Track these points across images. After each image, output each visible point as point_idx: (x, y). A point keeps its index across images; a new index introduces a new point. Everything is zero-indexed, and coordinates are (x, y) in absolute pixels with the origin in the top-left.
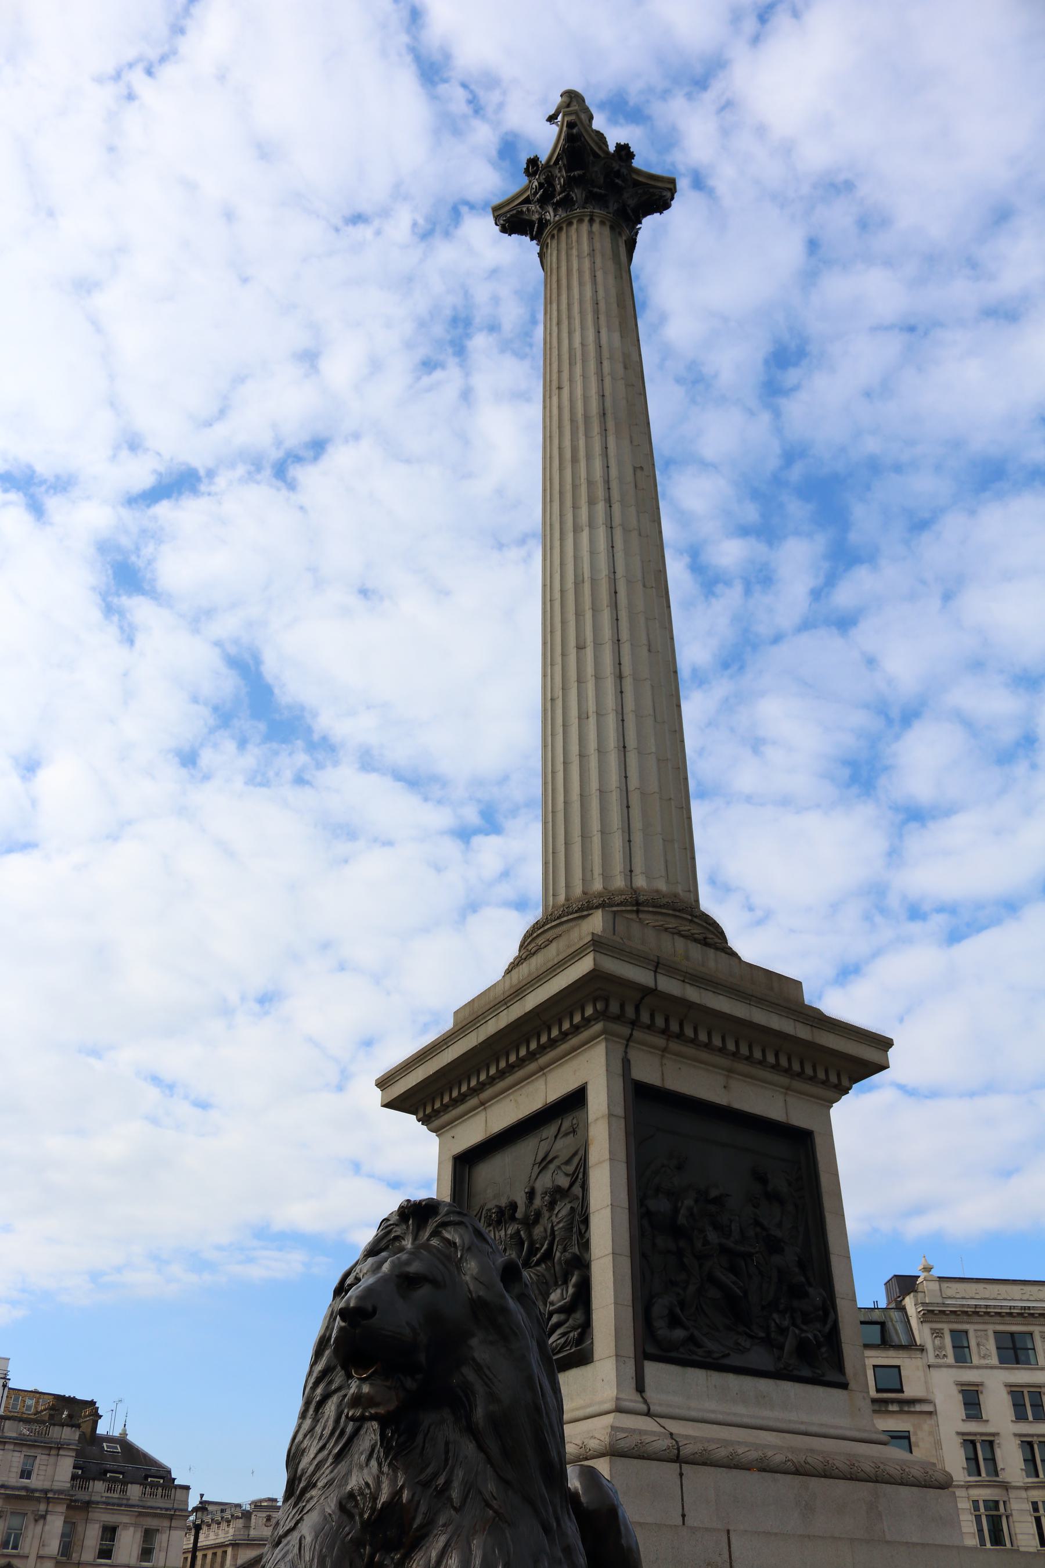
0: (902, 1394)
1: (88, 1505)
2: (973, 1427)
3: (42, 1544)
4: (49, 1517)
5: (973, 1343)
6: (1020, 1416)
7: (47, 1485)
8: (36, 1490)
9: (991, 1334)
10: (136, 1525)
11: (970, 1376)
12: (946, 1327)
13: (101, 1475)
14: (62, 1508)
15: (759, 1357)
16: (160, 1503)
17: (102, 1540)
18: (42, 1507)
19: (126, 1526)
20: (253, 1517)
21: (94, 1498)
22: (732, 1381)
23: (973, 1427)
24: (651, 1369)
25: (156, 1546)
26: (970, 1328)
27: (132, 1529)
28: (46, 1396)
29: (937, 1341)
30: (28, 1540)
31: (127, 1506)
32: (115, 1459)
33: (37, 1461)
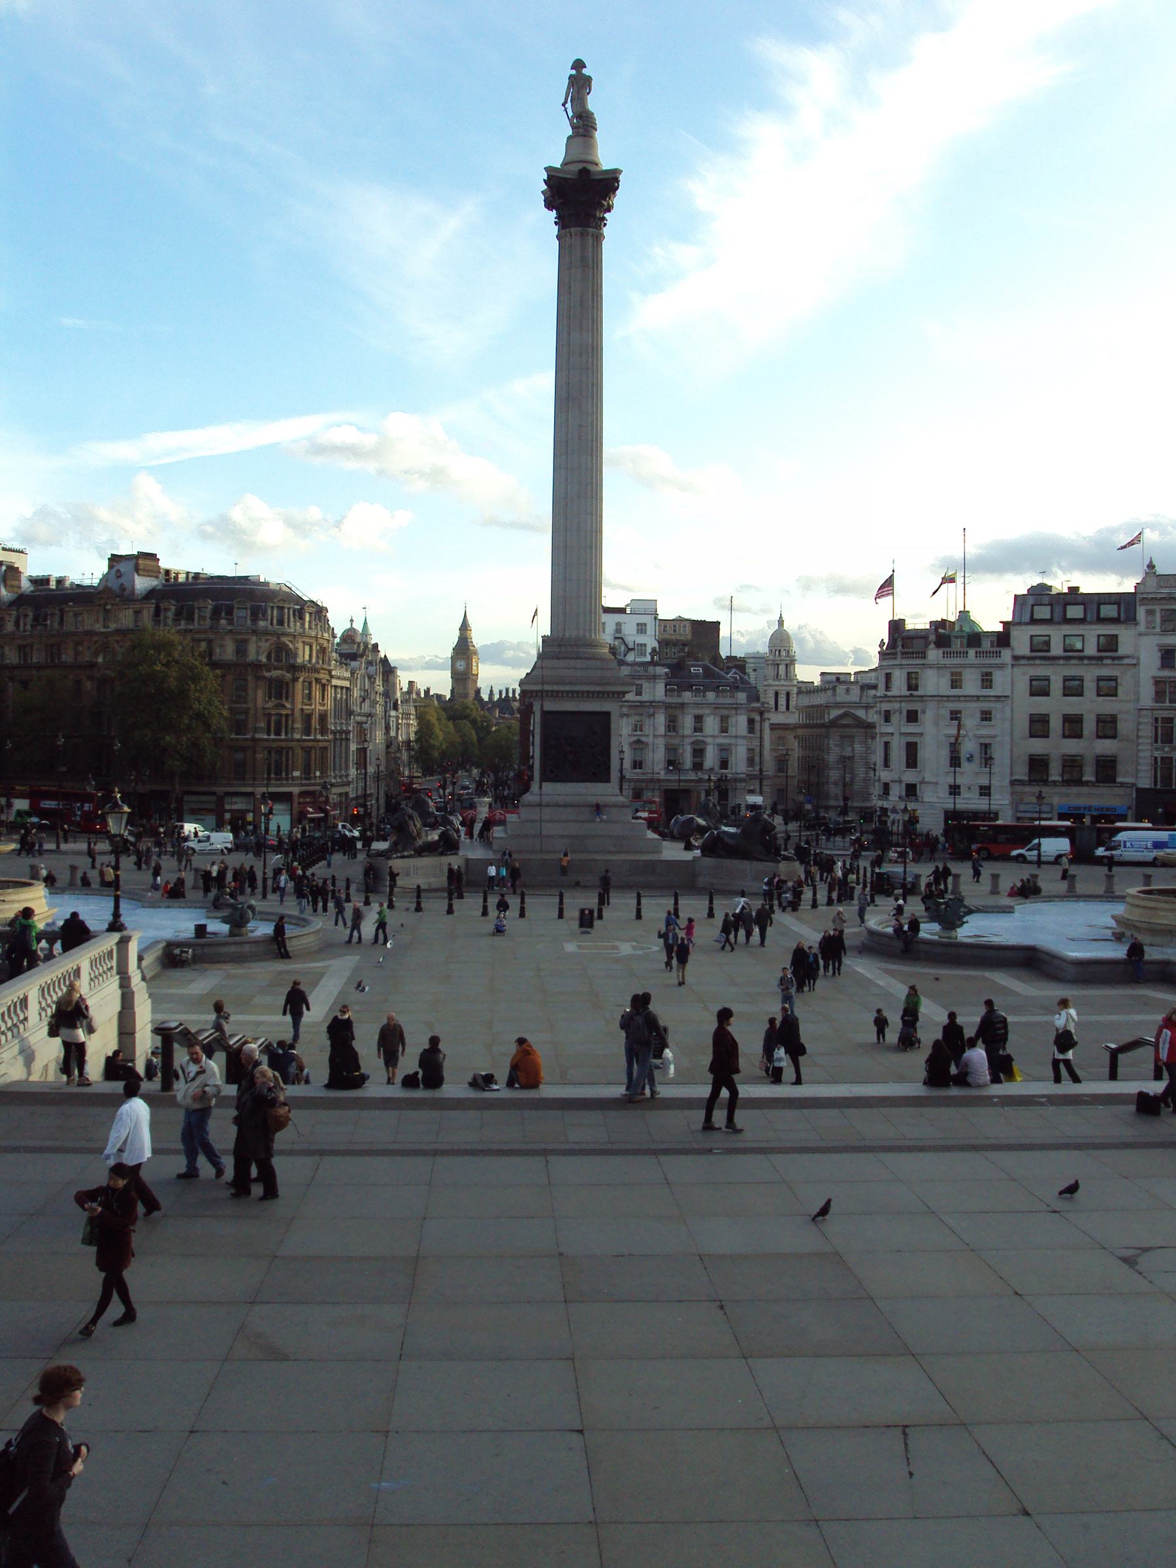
0: (1162, 642)
1: (682, 706)
2: (1166, 673)
3: (655, 729)
4: (656, 716)
7: (651, 699)
8: (646, 702)
10: (715, 714)
12: (1157, 608)
13: (689, 687)
14: (663, 710)
16: (729, 701)
17: (695, 722)
18: (651, 711)
19: (709, 715)
20: (837, 690)
21: (685, 701)
24: (544, 784)
25: (730, 724)
27: (712, 717)
28: (685, 622)
30: (647, 727)
31: (706, 704)
33: (644, 686)
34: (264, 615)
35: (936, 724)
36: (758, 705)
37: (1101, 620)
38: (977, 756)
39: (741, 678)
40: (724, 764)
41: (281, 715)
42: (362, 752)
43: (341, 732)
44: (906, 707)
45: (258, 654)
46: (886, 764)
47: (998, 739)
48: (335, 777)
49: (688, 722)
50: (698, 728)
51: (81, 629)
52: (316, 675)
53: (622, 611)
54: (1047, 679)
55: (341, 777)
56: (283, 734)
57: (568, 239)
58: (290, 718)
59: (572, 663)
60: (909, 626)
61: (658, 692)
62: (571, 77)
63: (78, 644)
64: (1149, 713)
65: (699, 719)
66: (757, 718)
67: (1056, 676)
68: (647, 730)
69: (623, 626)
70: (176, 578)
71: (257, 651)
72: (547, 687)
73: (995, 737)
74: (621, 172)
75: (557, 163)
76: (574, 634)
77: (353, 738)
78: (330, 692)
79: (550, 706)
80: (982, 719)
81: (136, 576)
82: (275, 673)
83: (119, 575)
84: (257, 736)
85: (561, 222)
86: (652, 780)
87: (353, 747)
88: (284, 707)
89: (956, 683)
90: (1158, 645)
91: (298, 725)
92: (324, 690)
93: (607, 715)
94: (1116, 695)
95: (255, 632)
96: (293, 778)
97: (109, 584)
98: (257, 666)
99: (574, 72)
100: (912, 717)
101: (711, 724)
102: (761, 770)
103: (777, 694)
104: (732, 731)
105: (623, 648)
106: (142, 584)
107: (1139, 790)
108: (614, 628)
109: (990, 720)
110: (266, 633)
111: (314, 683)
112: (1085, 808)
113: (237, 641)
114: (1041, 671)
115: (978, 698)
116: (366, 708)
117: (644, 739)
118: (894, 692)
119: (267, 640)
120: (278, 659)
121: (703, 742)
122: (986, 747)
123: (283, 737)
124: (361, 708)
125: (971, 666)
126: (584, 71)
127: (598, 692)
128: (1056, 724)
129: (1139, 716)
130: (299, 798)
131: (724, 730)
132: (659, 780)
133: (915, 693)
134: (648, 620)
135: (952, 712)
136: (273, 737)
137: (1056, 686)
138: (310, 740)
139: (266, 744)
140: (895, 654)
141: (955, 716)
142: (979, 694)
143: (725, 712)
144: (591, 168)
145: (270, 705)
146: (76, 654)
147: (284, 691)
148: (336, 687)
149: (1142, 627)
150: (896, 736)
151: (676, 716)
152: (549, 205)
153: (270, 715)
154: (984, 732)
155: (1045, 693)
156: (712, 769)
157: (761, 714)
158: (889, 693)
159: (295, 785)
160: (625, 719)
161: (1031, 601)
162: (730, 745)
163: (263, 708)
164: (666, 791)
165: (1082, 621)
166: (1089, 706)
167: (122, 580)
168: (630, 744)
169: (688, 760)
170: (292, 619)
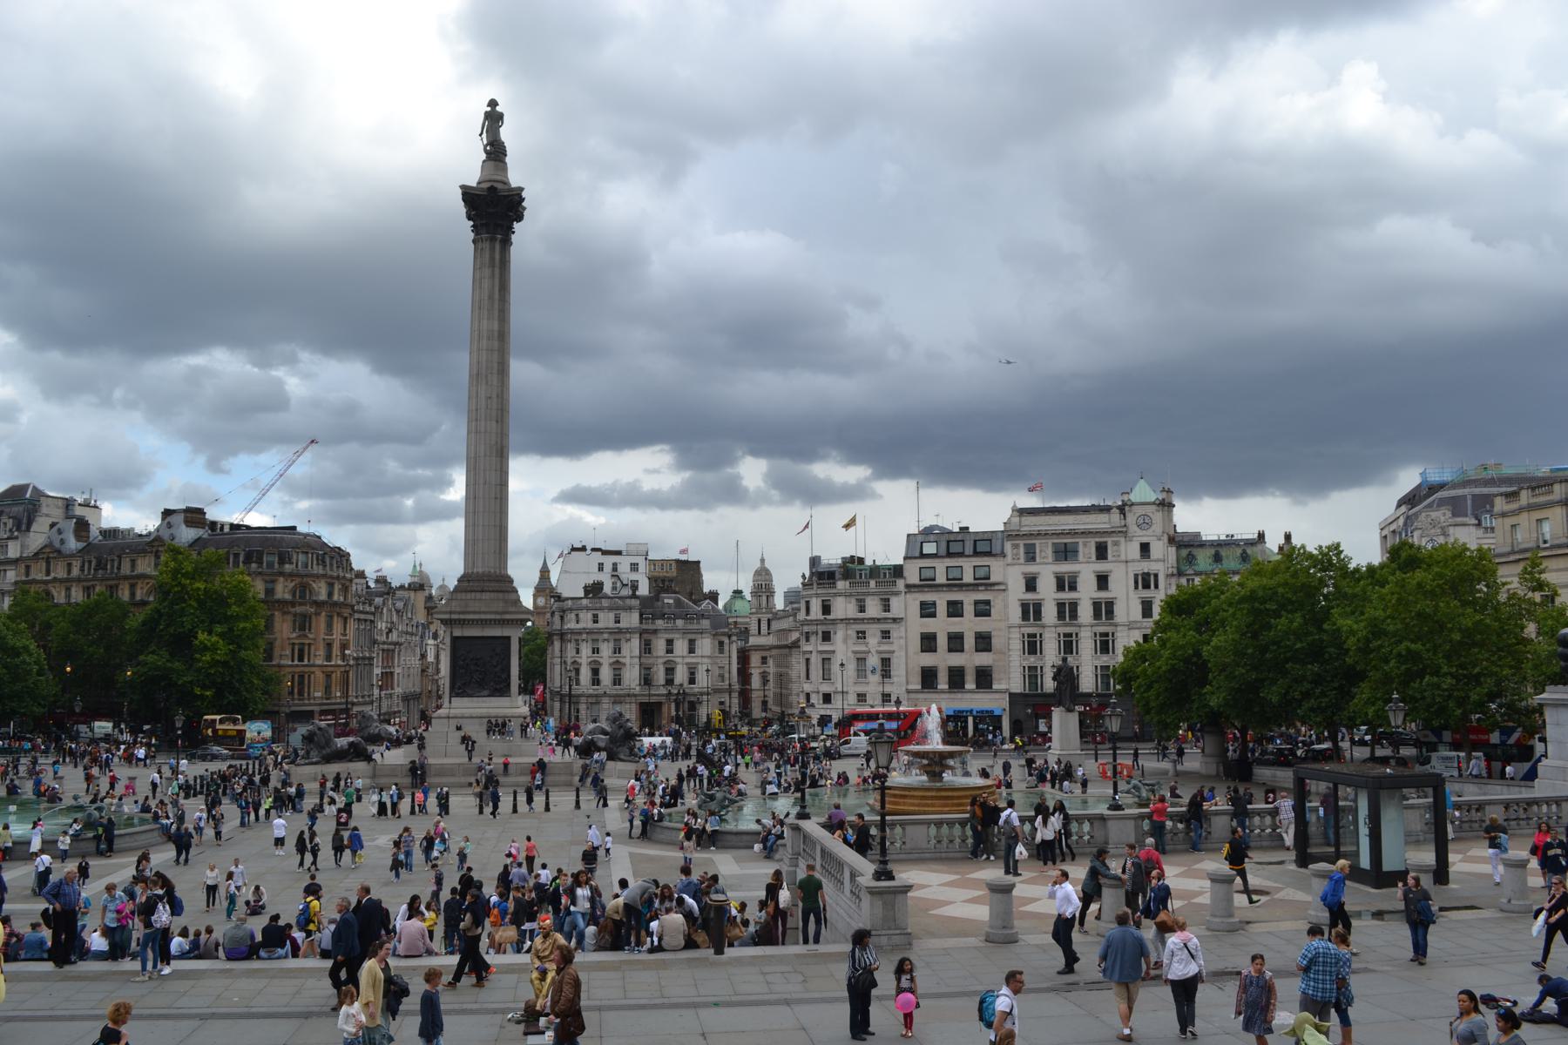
1: (655, 632)
2: (1030, 596)
5: (1037, 551)
6: (1060, 587)
7: (628, 626)
9: (1050, 545)
11: (1032, 569)
12: (1021, 543)
13: (662, 616)
15: (486, 693)
16: (695, 627)
18: (628, 635)
22: (475, 699)
23: (1030, 596)
26: (1037, 542)
29: (1015, 551)
32: (669, 607)
34: (290, 560)
35: (845, 640)
36: (726, 630)
37: (976, 554)
38: (879, 668)
39: (713, 607)
40: (692, 681)
41: (303, 644)
42: (387, 677)
43: (364, 658)
44: (821, 629)
45: (284, 592)
46: (808, 678)
47: (895, 655)
48: (357, 697)
49: (659, 645)
50: (670, 651)
51: (136, 573)
52: (338, 609)
53: (619, 553)
54: (934, 604)
55: (363, 697)
56: (306, 660)
57: (480, 243)
58: (313, 648)
59: (478, 595)
60: (824, 561)
61: (631, 620)
62: (486, 112)
63: (133, 587)
64: (1017, 630)
65: (670, 642)
66: (726, 641)
67: (941, 600)
68: (625, 650)
69: (619, 566)
70: (222, 528)
71: (282, 590)
72: (454, 616)
73: (893, 652)
74: (521, 189)
75: (472, 181)
76: (480, 570)
77: (378, 662)
78: (352, 625)
79: (458, 633)
80: (883, 638)
81: (184, 526)
82: (298, 609)
83: (169, 526)
84: (283, 662)
85: (475, 229)
86: (629, 695)
87: (377, 671)
88: (306, 636)
89: (862, 609)
90: (1023, 573)
91: (321, 652)
92: (345, 623)
93: (508, 638)
94: (990, 615)
95: (281, 574)
96: (315, 698)
97: (160, 533)
98: (282, 603)
99: (489, 109)
100: (826, 637)
101: (681, 646)
102: (730, 685)
103: (759, 621)
104: (698, 651)
105: (619, 584)
106: (187, 535)
107: (1011, 695)
108: (611, 566)
109: (889, 638)
110: (291, 575)
111: (335, 618)
112: (967, 712)
113: (266, 582)
114: (929, 597)
115: (878, 620)
116: (394, 637)
117: (621, 660)
118: (813, 616)
119: (292, 581)
120: (303, 596)
121: (675, 662)
122: (886, 662)
123: (306, 662)
124: (387, 637)
125: (873, 594)
126: (498, 108)
127: (499, 620)
128: (942, 642)
129: (1009, 632)
130: (320, 715)
131: (692, 651)
132: (635, 695)
133: (828, 617)
134: (640, 560)
135: (858, 632)
136: (296, 662)
137: (942, 609)
138: (331, 666)
139: (291, 670)
140: (812, 584)
141: (861, 635)
142: (879, 617)
143: (693, 636)
144: (499, 186)
145: (294, 635)
146: (133, 594)
147: (307, 625)
148: (359, 620)
149: (1009, 559)
150: (814, 654)
151: (650, 640)
152: (469, 218)
153: (294, 644)
154: (885, 648)
155: (933, 615)
156: (681, 685)
157: (730, 637)
158: (808, 618)
159: (316, 705)
160: (606, 643)
161: (920, 538)
162: (698, 663)
163: (289, 639)
164: (641, 704)
165: (961, 555)
166: (969, 625)
167: (172, 531)
168: (610, 665)
169: (660, 677)
170: (315, 562)
